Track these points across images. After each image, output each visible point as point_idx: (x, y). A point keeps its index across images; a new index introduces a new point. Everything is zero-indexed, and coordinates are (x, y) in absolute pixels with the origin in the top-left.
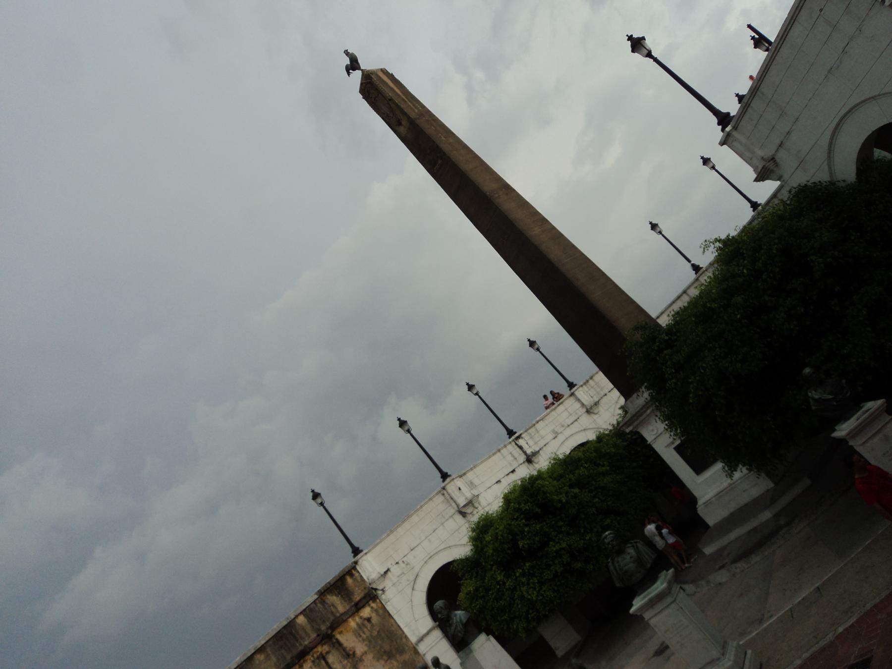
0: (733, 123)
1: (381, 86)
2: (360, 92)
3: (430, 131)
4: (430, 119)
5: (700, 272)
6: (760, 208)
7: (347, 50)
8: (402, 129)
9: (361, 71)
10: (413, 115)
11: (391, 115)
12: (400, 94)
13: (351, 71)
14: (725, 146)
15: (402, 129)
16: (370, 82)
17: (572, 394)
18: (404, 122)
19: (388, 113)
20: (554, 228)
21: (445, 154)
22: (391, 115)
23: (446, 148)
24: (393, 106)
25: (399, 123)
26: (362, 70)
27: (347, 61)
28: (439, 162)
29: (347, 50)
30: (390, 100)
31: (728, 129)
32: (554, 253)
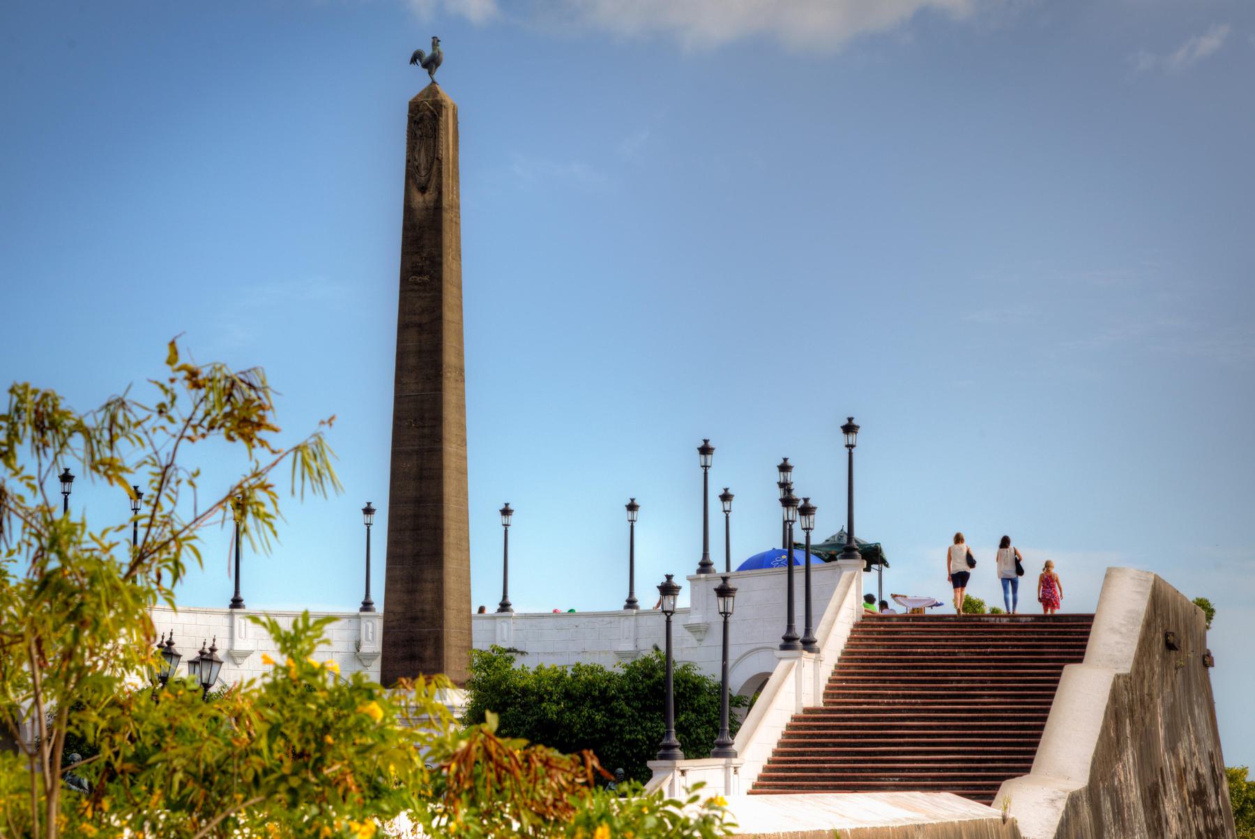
0: (709, 575)
1: (443, 132)
2: (410, 103)
3: (447, 238)
4: (454, 219)
5: (505, 614)
6: (635, 611)
7: (439, 41)
8: (419, 200)
9: (430, 81)
10: (445, 203)
11: (423, 173)
12: (451, 158)
13: (418, 61)
14: (689, 582)
15: (419, 200)
16: (435, 115)
17: (231, 614)
18: (429, 196)
19: (422, 166)
20: (465, 458)
21: (440, 279)
22: (423, 173)
23: (447, 275)
24: (435, 167)
25: (423, 190)
26: (434, 82)
27: (428, 53)
28: (426, 278)
29: (439, 41)
30: (438, 159)
31: (703, 576)
32: (450, 488)
